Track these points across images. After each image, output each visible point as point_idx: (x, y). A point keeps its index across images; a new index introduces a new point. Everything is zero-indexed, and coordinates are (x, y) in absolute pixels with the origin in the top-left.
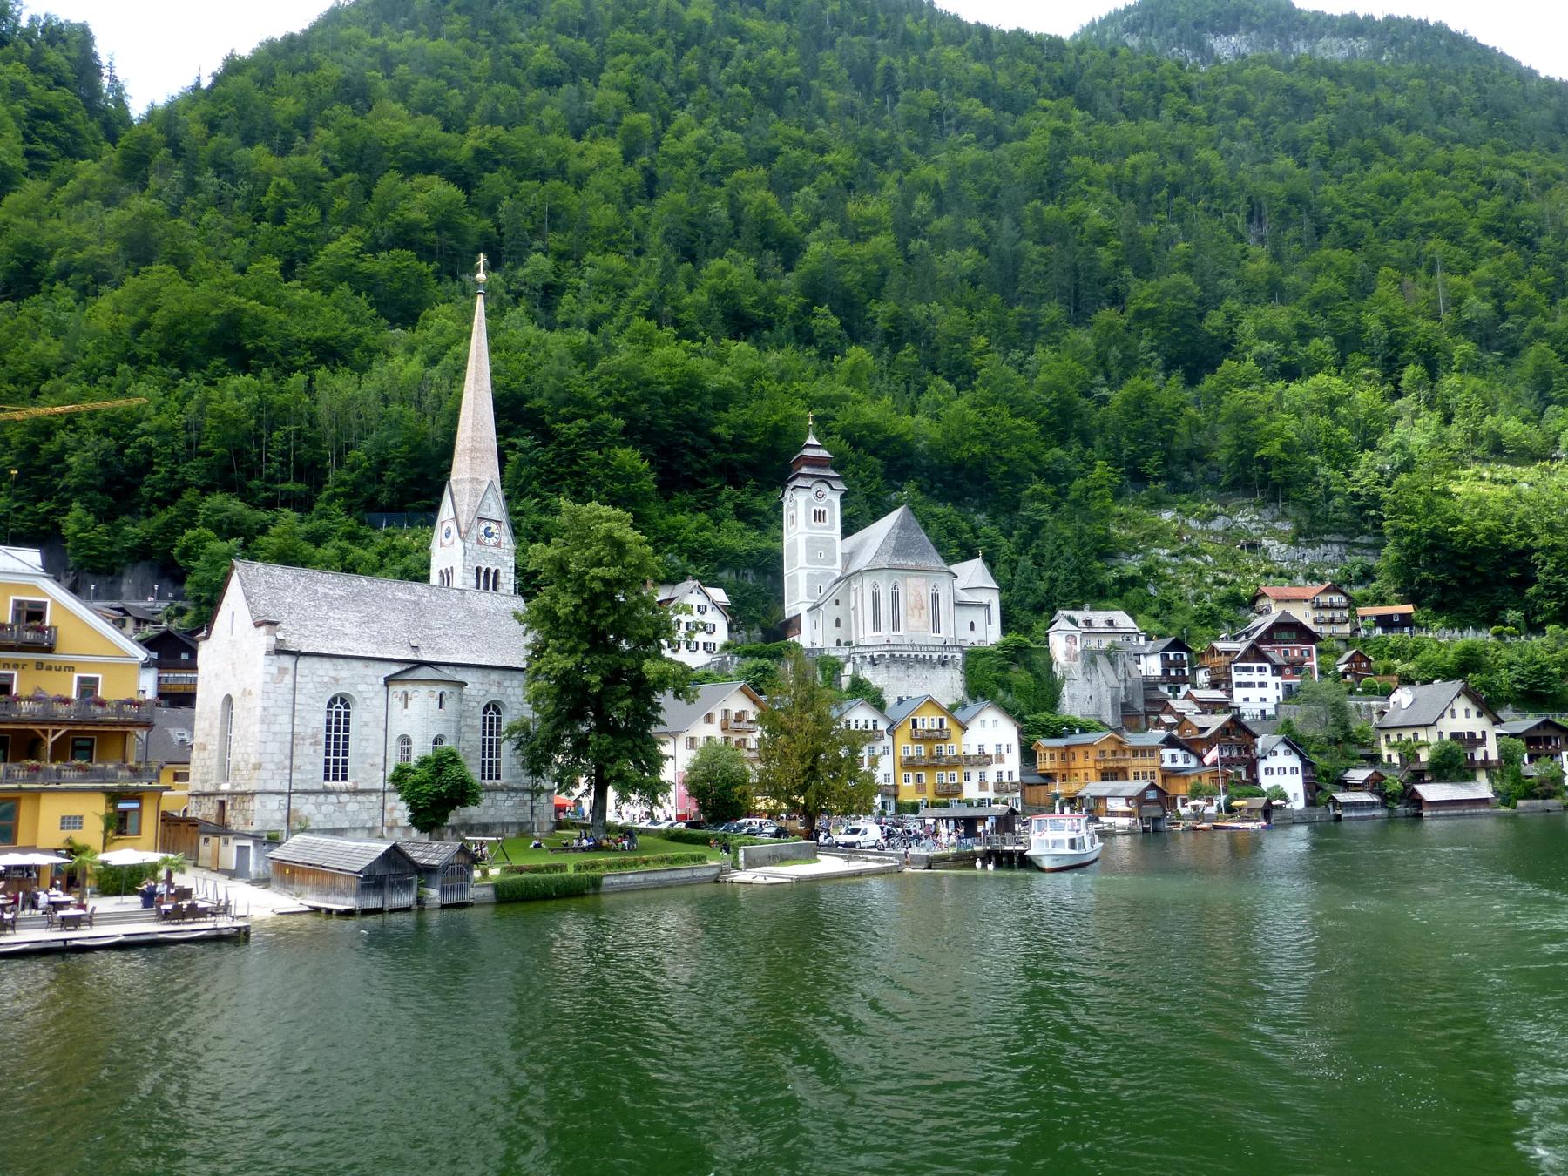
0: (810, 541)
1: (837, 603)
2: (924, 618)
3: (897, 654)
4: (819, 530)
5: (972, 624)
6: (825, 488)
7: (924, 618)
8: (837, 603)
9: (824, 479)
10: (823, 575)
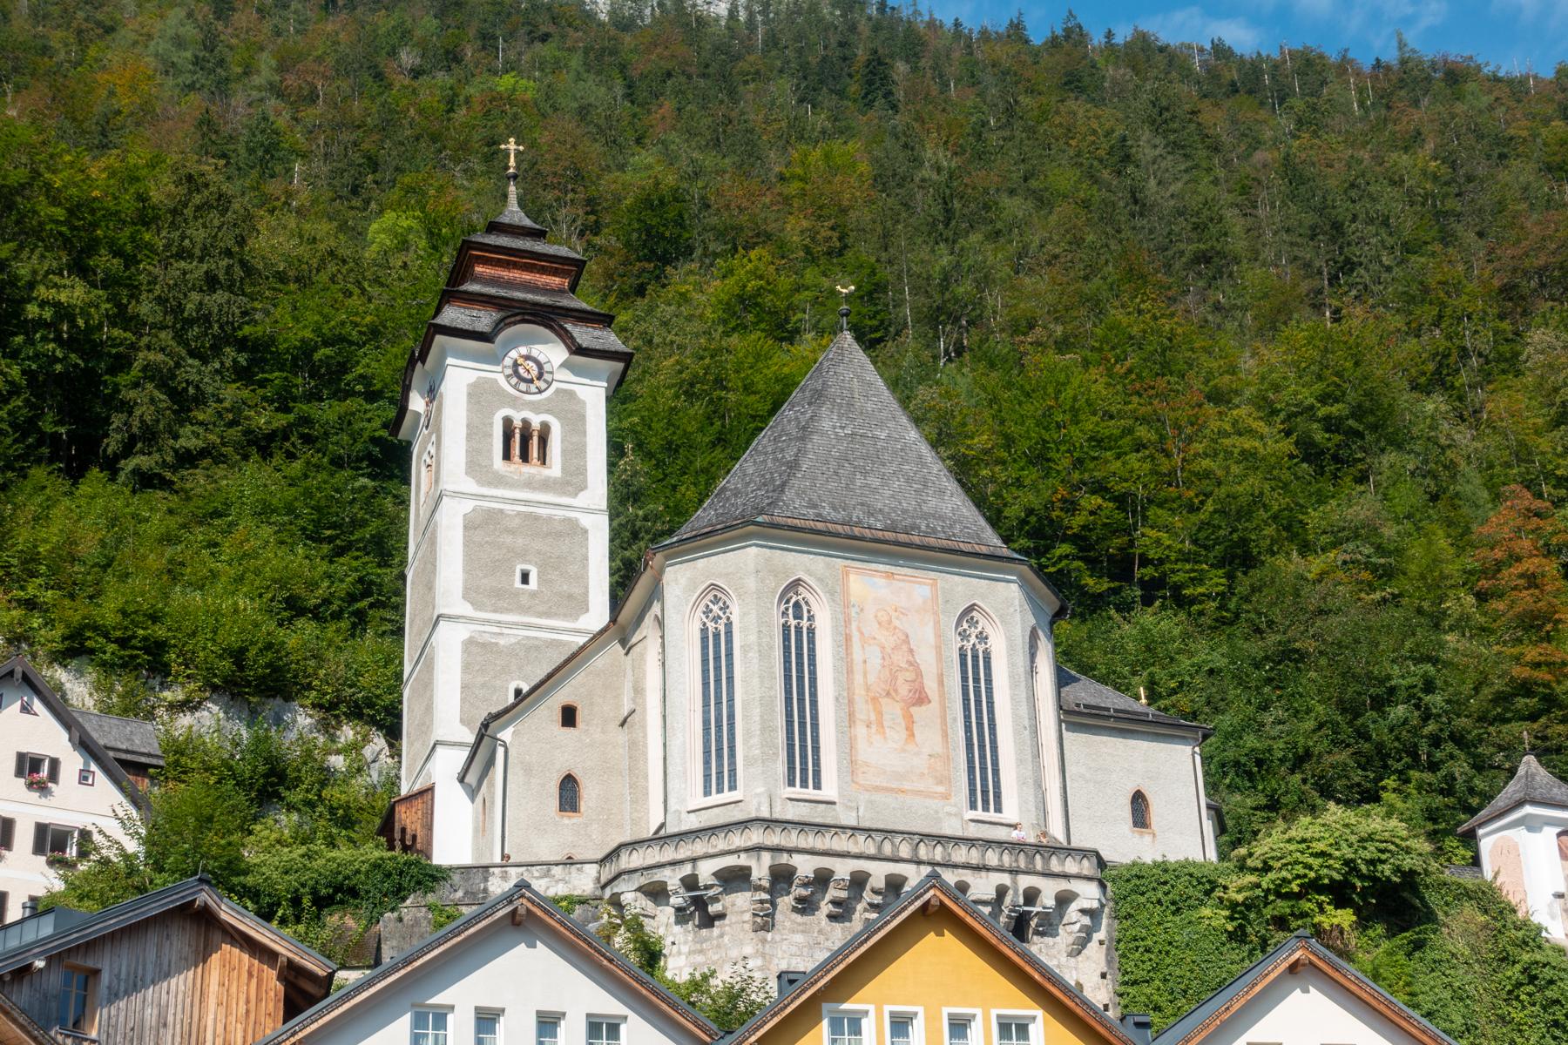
0: (479, 525)
1: (569, 716)
2: (928, 737)
3: (805, 866)
4: (520, 490)
5: (1139, 800)
6: (553, 353)
7: (928, 737)
8: (569, 716)
9: (549, 317)
10: (532, 649)
